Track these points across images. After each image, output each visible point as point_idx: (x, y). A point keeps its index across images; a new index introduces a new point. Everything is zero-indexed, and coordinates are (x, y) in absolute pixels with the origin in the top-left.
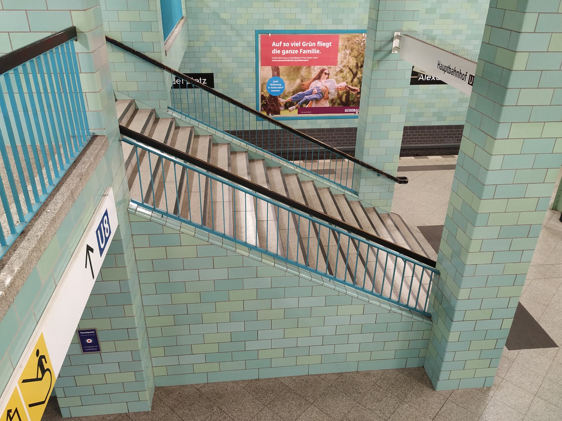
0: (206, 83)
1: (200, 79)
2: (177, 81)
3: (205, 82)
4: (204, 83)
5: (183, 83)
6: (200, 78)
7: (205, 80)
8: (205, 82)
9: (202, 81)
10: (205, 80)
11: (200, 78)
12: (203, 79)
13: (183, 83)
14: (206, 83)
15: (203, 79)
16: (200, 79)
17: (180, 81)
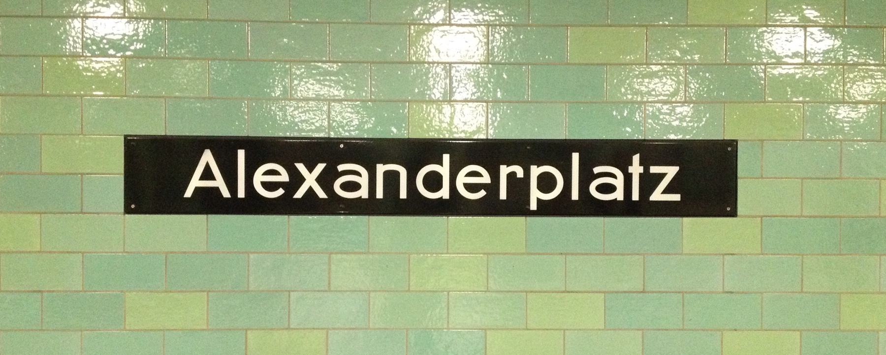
0: (676, 197)
1: (636, 169)
2: (462, 179)
3: (664, 192)
4: (657, 195)
5: (503, 195)
6: (636, 158)
7: (671, 171)
8: (665, 192)
9: (649, 182)
10: (671, 171)
11: (636, 158)
12: (654, 170)
13: (503, 195)
14: (676, 197)
15: (654, 170)
16: (636, 169)
17: (486, 179)
